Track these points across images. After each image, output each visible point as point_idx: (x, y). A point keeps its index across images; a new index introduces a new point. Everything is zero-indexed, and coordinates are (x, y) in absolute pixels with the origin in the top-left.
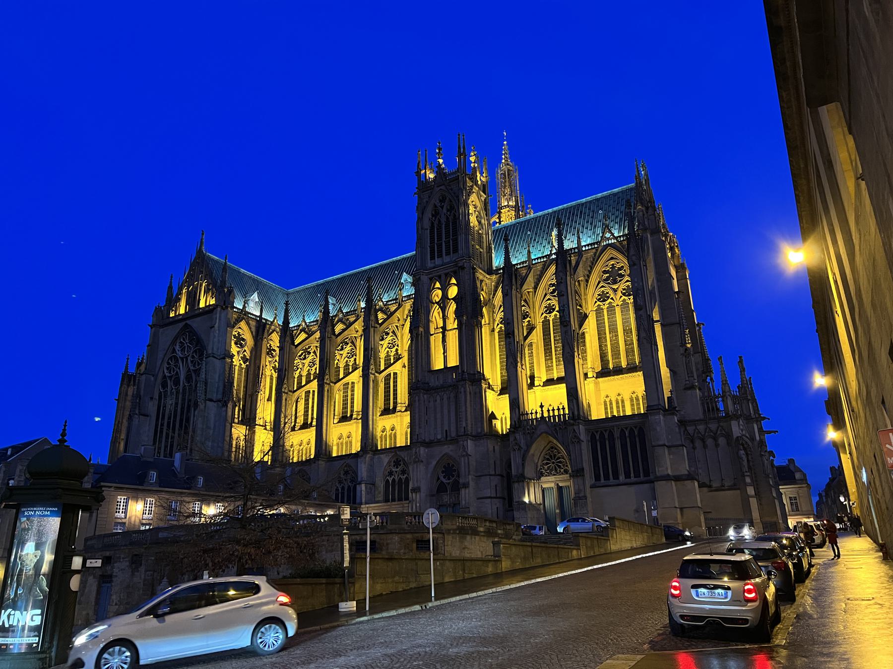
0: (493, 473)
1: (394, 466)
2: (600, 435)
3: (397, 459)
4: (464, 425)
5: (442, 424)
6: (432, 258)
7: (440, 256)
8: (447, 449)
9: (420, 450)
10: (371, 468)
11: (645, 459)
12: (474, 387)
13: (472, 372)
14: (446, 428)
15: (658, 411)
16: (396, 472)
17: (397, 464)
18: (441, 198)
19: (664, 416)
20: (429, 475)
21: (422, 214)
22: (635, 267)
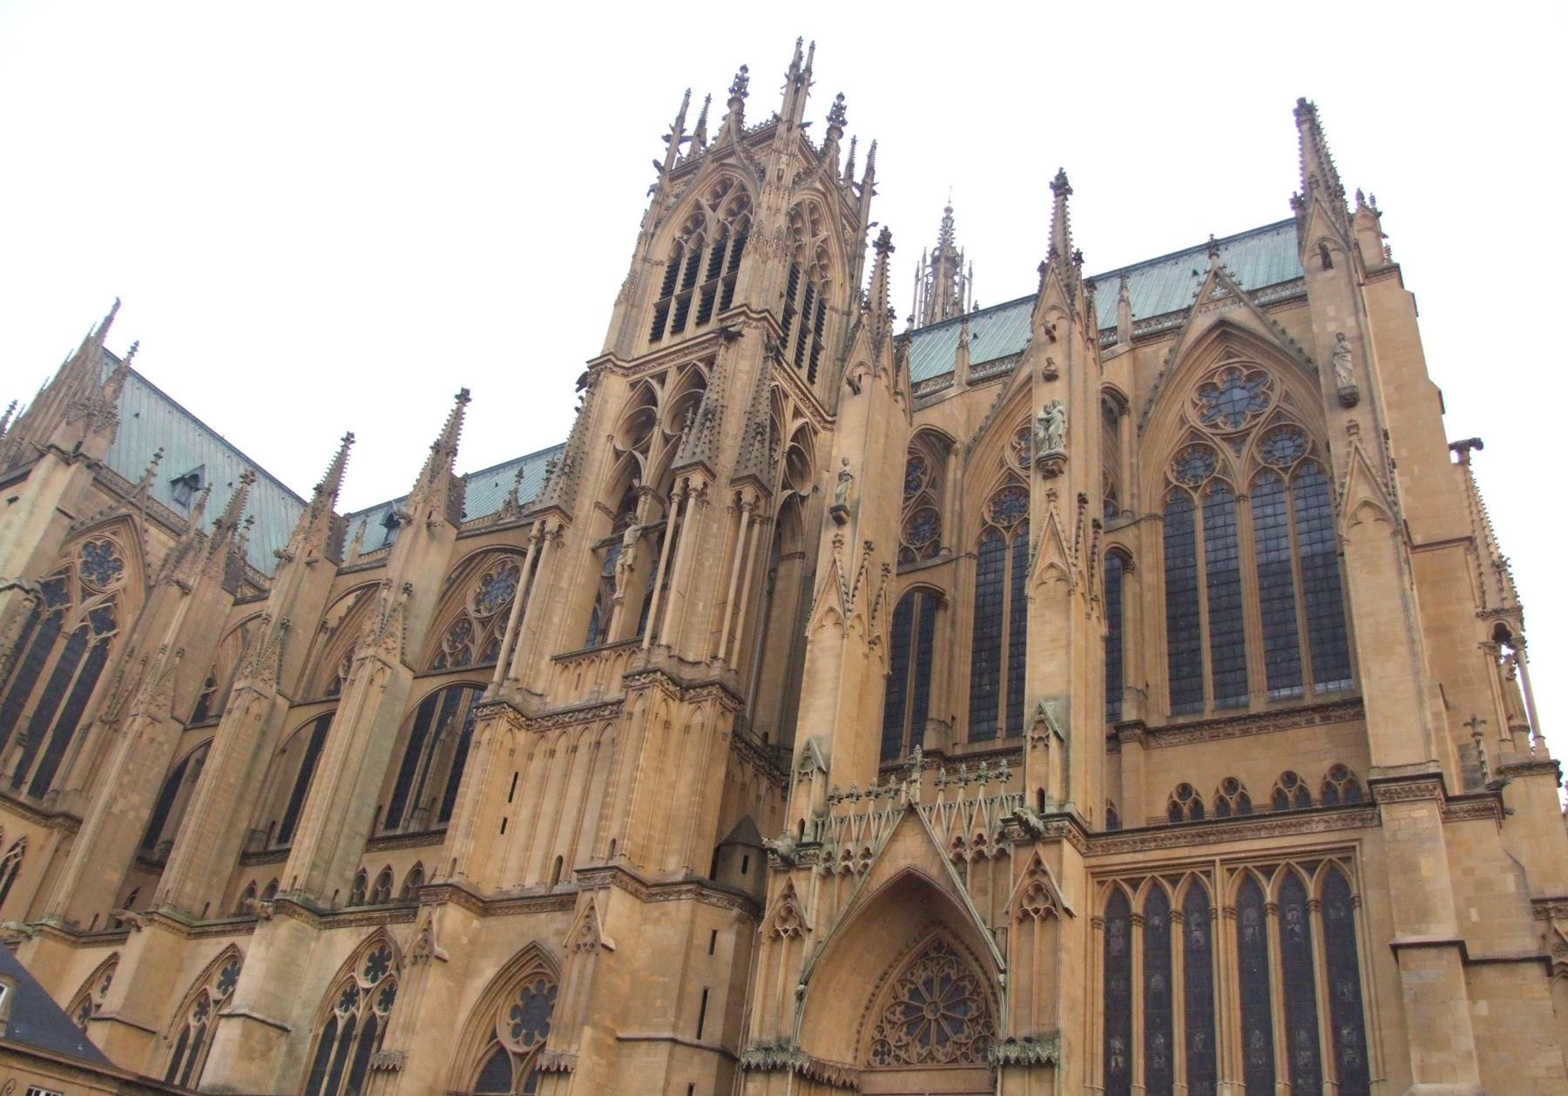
0: (689, 1036)
1: (367, 973)
2: (1148, 900)
3: (382, 950)
4: (614, 830)
5: (553, 835)
6: (657, 335)
7: (679, 327)
8: (548, 928)
9: (441, 920)
10: (284, 973)
11: (1348, 1011)
12: (686, 708)
13: (691, 657)
14: (561, 849)
15: (1422, 784)
16: (367, 991)
17: (377, 966)
18: (718, 189)
19: (1447, 816)
20: (462, 1017)
21: (656, 227)
22: (1330, 273)
